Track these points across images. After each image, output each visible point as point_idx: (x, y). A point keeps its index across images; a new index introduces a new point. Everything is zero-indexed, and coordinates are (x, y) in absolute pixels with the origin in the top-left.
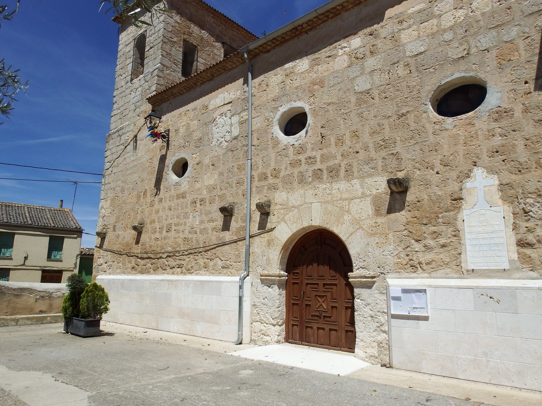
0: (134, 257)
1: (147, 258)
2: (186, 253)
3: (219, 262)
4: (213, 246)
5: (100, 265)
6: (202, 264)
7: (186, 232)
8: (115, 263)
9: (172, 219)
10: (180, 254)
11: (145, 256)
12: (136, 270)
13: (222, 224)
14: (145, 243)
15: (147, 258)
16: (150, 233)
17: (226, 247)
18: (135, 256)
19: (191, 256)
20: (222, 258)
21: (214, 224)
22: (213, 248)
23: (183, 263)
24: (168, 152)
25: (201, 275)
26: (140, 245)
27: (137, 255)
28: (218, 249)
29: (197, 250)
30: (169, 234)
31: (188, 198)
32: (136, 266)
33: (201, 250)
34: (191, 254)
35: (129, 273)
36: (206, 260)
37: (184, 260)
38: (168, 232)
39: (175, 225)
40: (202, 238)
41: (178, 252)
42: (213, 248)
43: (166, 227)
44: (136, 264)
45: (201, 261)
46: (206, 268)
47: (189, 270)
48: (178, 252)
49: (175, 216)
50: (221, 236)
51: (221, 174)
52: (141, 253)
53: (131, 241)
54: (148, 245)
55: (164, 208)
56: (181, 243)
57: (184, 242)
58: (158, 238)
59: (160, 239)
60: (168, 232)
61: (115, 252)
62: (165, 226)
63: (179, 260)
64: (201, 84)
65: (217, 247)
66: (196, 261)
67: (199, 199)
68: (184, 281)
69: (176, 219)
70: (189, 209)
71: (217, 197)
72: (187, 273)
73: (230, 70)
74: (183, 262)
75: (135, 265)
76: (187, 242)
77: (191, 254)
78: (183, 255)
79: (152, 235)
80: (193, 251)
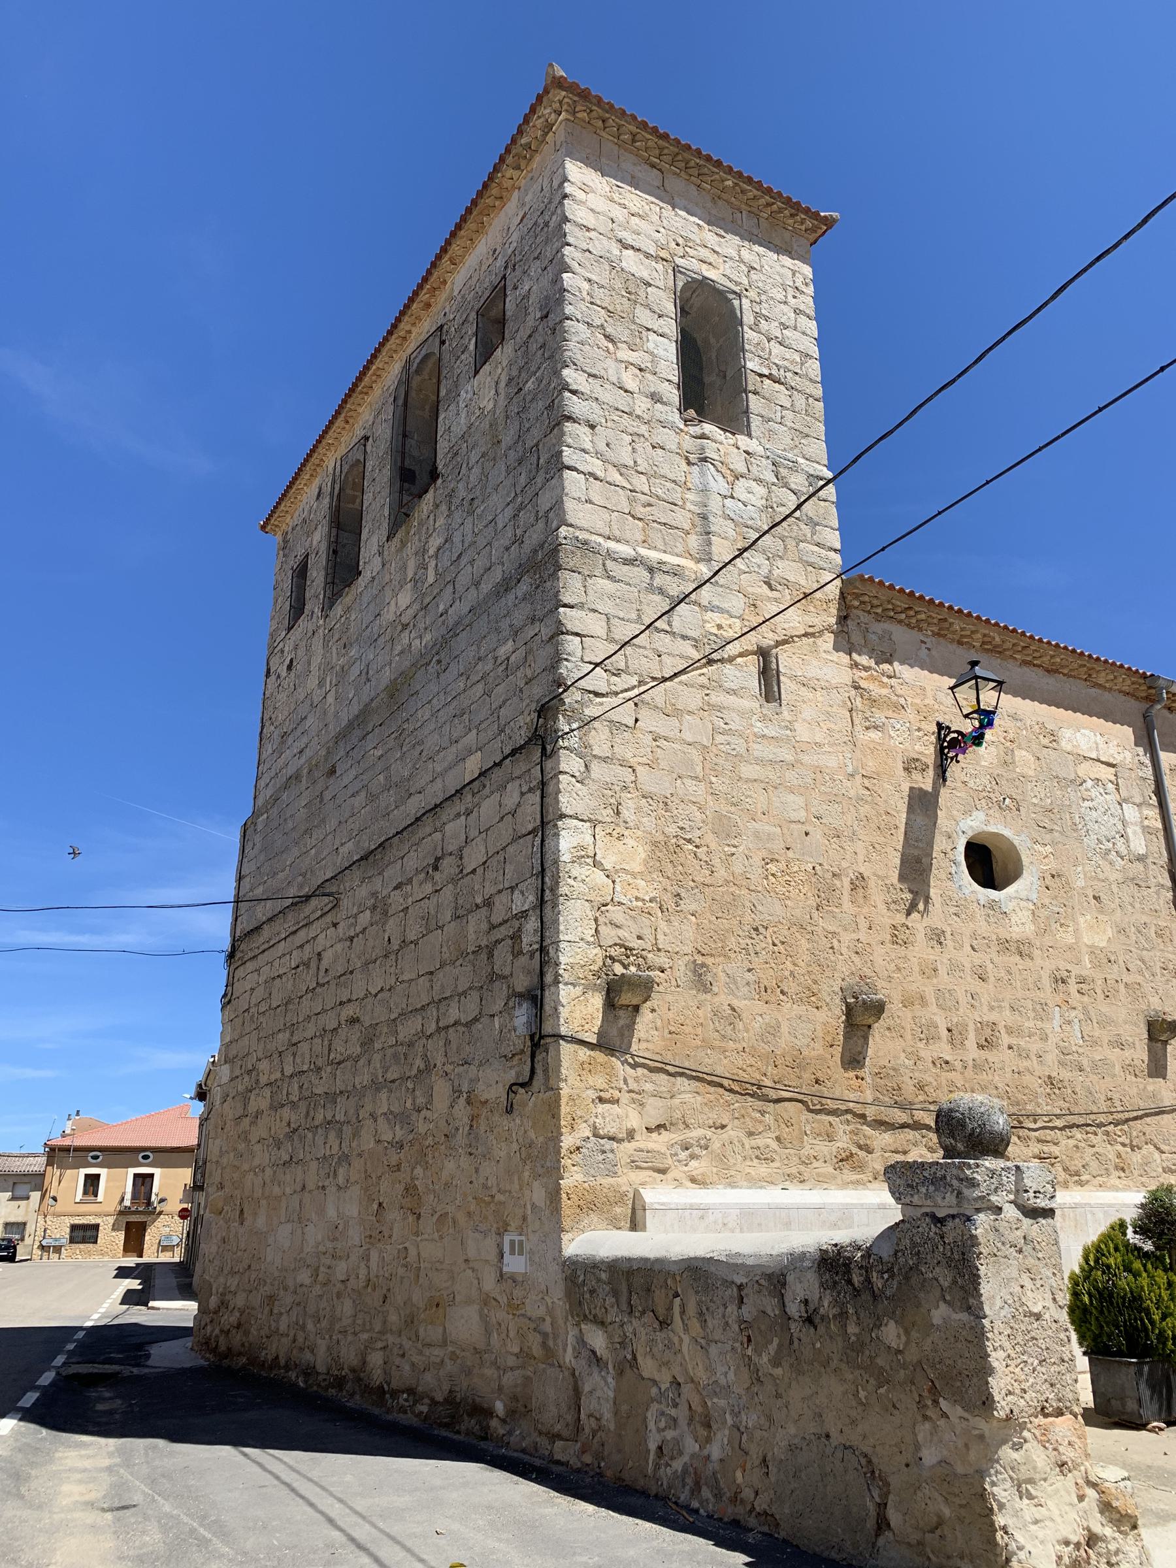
0: (849, 1117)
1: (904, 1126)
2: (1059, 1123)
3: (1157, 1155)
4: (1135, 1114)
5: (623, 1135)
6: (1112, 1156)
7: (1052, 1057)
8: (731, 1133)
9: (992, 1008)
10: (1039, 1125)
11: (901, 1117)
12: (860, 1167)
13: (1146, 1059)
14: (894, 1069)
15: (904, 1126)
16: (908, 1037)
17: (1165, 1116)
18: (848, 1111)
19: (1078, 1134)
20: (1164, 1147)
21: (1128, 1053)
22: (1136, 1118)
23: (1058, 1154)
24: (944, 793)
25: (1115, 1189)
26: (866, 1072)
27: (859, 1109)
28: (1148, 1120)
29: (1093, 1117)
30: (991, 1056)
31: (1038, 961)
32: (861, 1153)
33: (1102, 1119)
34: (1078, 1126)
35: (821, 1181)
36: (1119, 1147)
37: (1056, 1144)
38: (983, 1047)
39: (1010, 1031)
40: (1101, 1087)
41: (1031, 1118)
42: (1136, 1118)
43: (976, 1030)
44: (860, 1147)
45: (1110, 1152)
46: (1123, 1170)
47: (1077, 1174)
48: (1035, 1117)
49: (1006, 1004)
50: (1150, 1088)
51: (1122, 931)
52: (876, 1102)
53: (819, 1049)
54: (906, 1079)
55: (955, 968)
56: (1039, 1090)
57: (1048, 1090)
58: (947, 1062)
59: (958, 1065)
60: (983, 1047)
61: (726, 1083)
62: (971, 1027)
63: (1039, 1141)
64: (1025, 663)
65: (1147, 1115)
66: (1094, 1150)
67: (1073, 974)
68: (1101, 1206)
69: (1007, 1012)
70: (1047, 993)
71: (1122, 987)
72: (1071, 1184)
73: (1097, 685)
74: (1055, 1150)
75: (855, 1150)
76: (1057, 1091)
77: (1078, 1126)
78: (1052, 1128)
79: (921, 1045)
80: (1081, 1121)
